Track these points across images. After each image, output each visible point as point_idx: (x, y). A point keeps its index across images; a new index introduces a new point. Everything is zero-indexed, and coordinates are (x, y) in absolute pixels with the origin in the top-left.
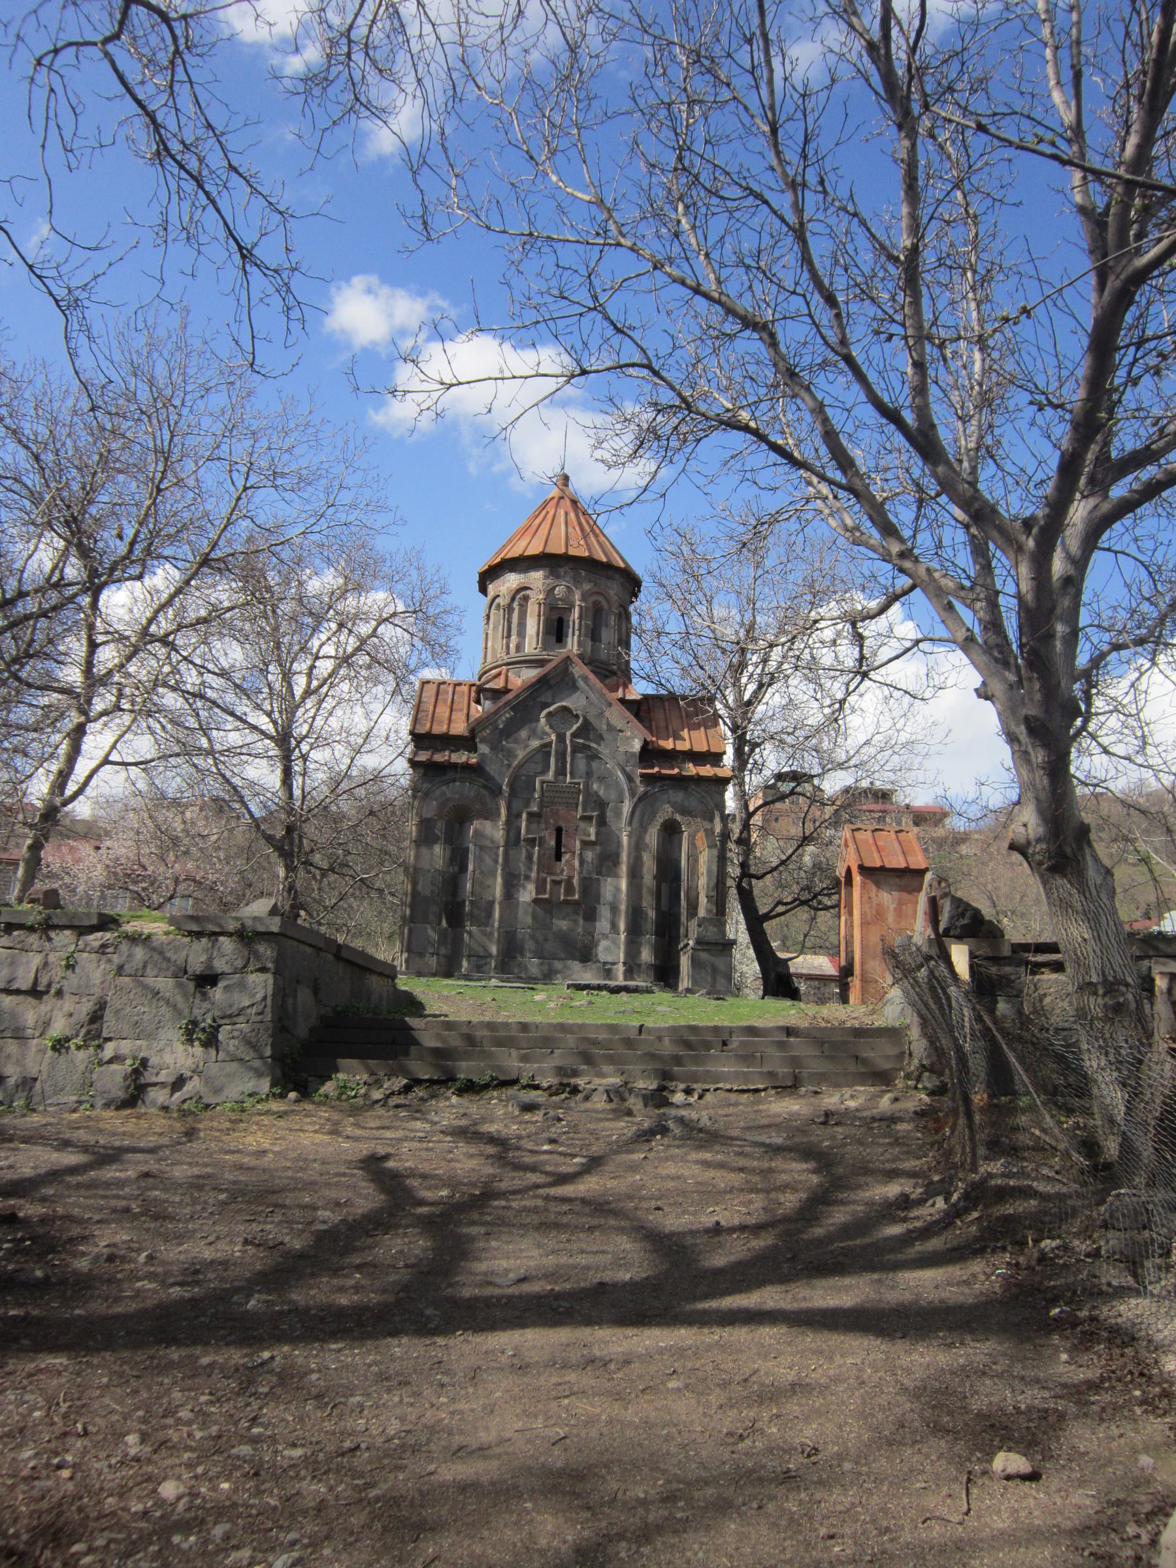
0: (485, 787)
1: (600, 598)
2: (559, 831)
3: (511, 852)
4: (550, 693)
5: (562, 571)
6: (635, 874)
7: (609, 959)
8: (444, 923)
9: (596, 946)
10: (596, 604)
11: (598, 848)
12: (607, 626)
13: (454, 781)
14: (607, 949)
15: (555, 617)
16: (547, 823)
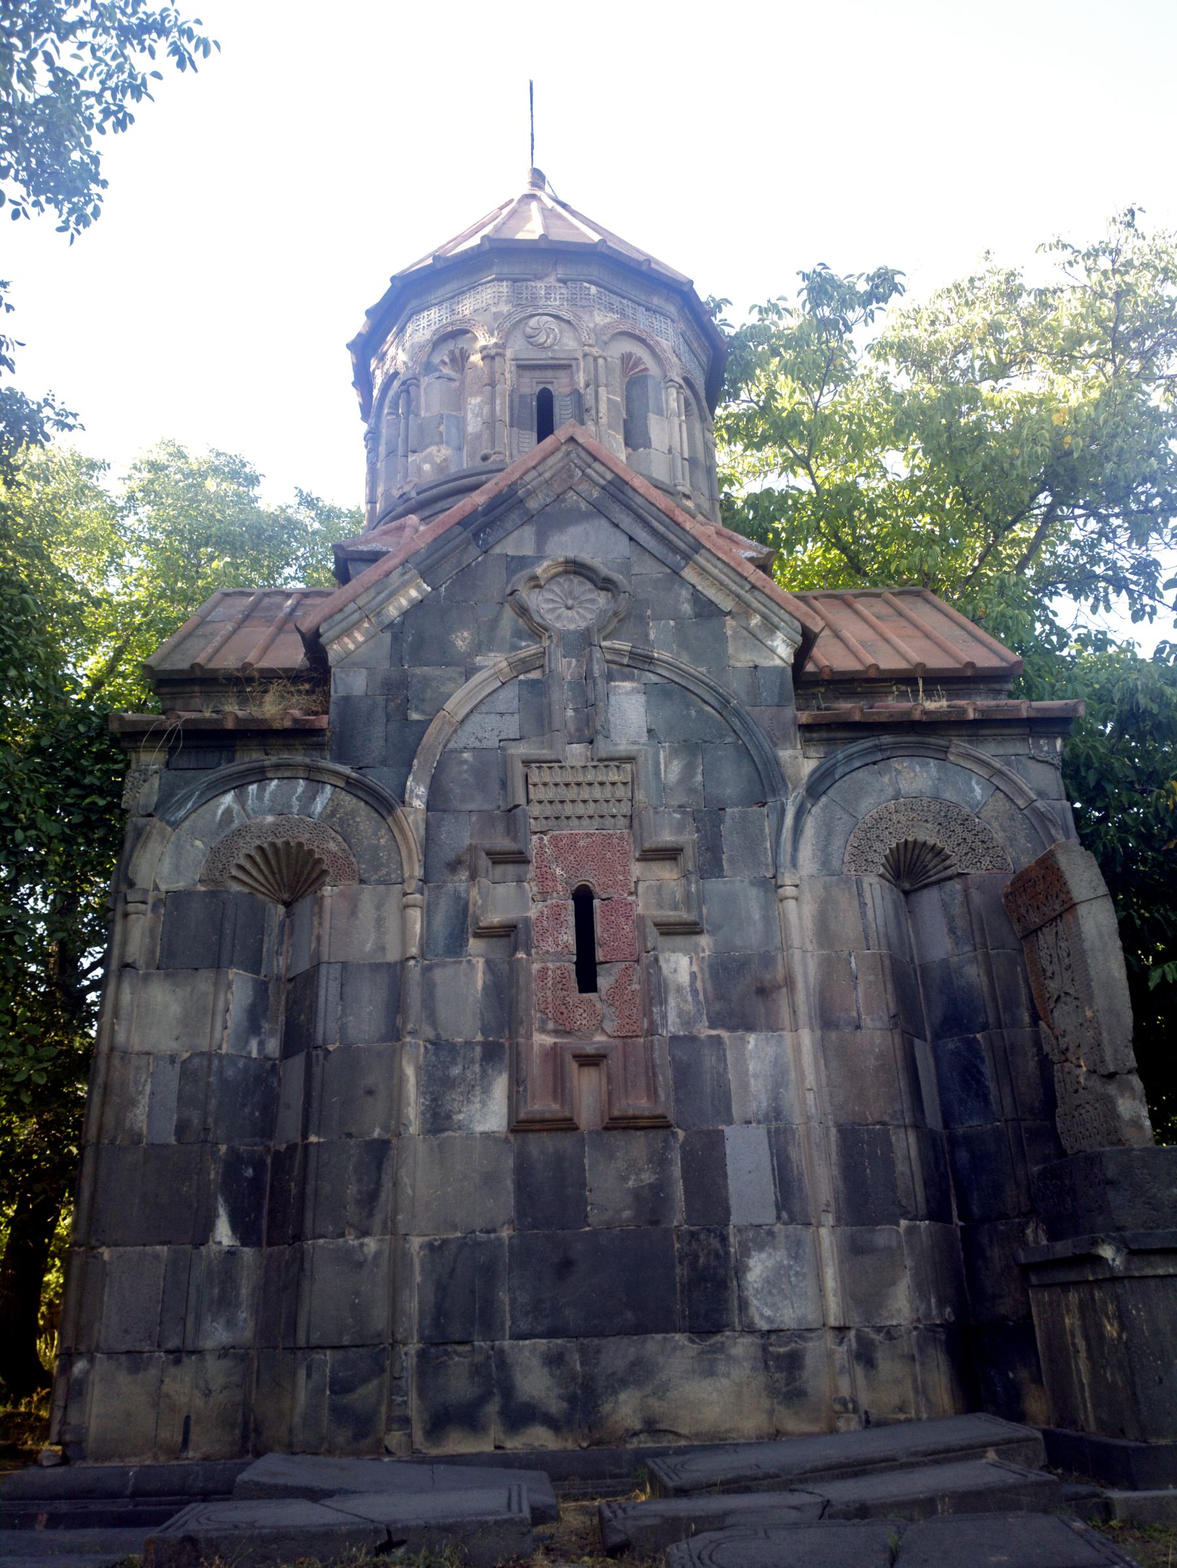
0: (352, 786)
1: (639, 351)
2: (583, 899)
3: (438, 975)
4: (529, 532)
5: (540, 287)
6: (826, 1020)
7: (789, 1316)
8: (223, 1233)
9: (741, 1270)
10: (626, 358)
11: (705, 941)
12: (660, 412)
13: (260, 775)
14: (772, 1283)
15: (531, 386)
16: (542, 878)
